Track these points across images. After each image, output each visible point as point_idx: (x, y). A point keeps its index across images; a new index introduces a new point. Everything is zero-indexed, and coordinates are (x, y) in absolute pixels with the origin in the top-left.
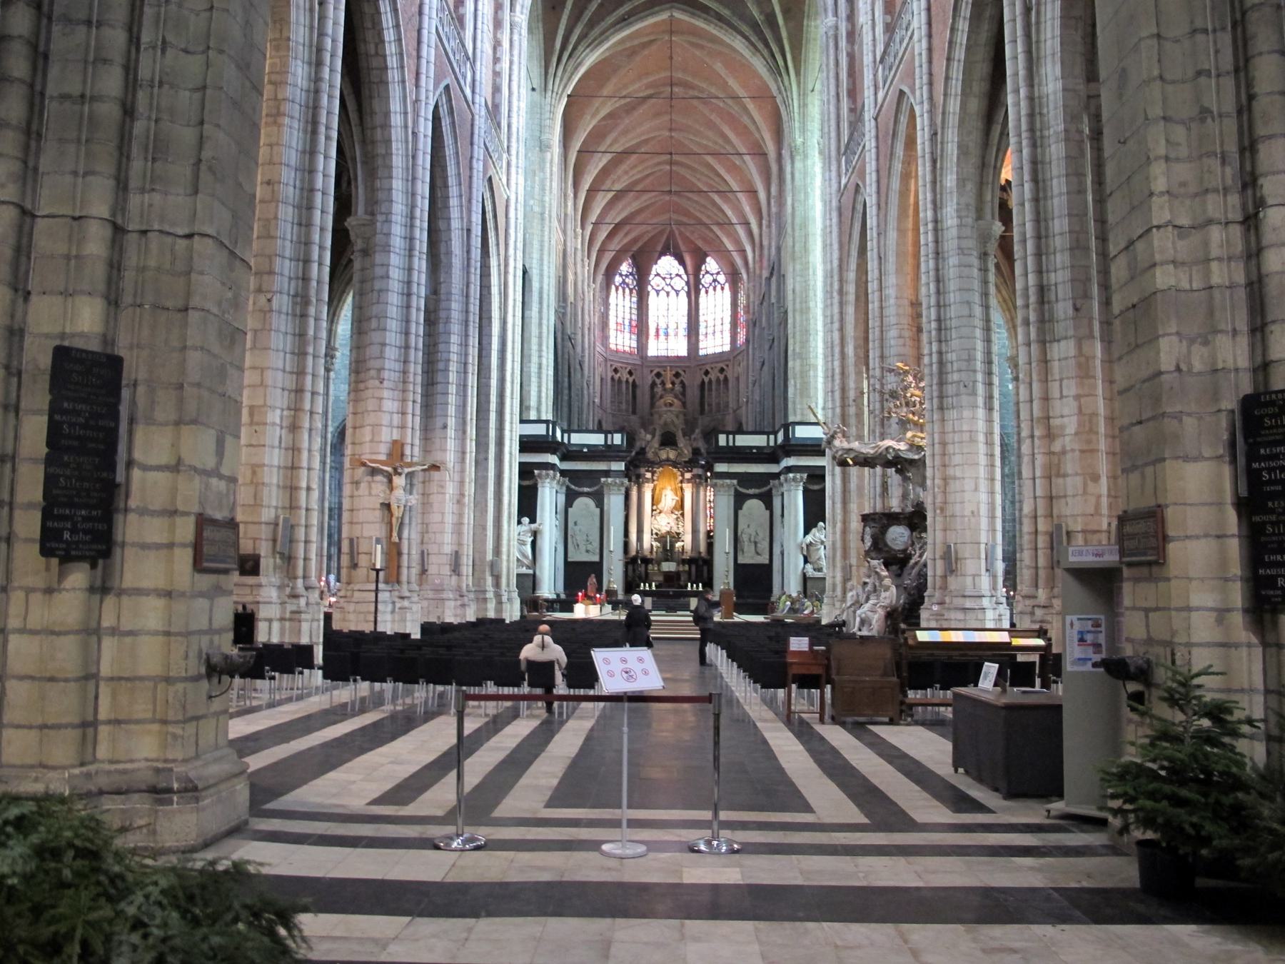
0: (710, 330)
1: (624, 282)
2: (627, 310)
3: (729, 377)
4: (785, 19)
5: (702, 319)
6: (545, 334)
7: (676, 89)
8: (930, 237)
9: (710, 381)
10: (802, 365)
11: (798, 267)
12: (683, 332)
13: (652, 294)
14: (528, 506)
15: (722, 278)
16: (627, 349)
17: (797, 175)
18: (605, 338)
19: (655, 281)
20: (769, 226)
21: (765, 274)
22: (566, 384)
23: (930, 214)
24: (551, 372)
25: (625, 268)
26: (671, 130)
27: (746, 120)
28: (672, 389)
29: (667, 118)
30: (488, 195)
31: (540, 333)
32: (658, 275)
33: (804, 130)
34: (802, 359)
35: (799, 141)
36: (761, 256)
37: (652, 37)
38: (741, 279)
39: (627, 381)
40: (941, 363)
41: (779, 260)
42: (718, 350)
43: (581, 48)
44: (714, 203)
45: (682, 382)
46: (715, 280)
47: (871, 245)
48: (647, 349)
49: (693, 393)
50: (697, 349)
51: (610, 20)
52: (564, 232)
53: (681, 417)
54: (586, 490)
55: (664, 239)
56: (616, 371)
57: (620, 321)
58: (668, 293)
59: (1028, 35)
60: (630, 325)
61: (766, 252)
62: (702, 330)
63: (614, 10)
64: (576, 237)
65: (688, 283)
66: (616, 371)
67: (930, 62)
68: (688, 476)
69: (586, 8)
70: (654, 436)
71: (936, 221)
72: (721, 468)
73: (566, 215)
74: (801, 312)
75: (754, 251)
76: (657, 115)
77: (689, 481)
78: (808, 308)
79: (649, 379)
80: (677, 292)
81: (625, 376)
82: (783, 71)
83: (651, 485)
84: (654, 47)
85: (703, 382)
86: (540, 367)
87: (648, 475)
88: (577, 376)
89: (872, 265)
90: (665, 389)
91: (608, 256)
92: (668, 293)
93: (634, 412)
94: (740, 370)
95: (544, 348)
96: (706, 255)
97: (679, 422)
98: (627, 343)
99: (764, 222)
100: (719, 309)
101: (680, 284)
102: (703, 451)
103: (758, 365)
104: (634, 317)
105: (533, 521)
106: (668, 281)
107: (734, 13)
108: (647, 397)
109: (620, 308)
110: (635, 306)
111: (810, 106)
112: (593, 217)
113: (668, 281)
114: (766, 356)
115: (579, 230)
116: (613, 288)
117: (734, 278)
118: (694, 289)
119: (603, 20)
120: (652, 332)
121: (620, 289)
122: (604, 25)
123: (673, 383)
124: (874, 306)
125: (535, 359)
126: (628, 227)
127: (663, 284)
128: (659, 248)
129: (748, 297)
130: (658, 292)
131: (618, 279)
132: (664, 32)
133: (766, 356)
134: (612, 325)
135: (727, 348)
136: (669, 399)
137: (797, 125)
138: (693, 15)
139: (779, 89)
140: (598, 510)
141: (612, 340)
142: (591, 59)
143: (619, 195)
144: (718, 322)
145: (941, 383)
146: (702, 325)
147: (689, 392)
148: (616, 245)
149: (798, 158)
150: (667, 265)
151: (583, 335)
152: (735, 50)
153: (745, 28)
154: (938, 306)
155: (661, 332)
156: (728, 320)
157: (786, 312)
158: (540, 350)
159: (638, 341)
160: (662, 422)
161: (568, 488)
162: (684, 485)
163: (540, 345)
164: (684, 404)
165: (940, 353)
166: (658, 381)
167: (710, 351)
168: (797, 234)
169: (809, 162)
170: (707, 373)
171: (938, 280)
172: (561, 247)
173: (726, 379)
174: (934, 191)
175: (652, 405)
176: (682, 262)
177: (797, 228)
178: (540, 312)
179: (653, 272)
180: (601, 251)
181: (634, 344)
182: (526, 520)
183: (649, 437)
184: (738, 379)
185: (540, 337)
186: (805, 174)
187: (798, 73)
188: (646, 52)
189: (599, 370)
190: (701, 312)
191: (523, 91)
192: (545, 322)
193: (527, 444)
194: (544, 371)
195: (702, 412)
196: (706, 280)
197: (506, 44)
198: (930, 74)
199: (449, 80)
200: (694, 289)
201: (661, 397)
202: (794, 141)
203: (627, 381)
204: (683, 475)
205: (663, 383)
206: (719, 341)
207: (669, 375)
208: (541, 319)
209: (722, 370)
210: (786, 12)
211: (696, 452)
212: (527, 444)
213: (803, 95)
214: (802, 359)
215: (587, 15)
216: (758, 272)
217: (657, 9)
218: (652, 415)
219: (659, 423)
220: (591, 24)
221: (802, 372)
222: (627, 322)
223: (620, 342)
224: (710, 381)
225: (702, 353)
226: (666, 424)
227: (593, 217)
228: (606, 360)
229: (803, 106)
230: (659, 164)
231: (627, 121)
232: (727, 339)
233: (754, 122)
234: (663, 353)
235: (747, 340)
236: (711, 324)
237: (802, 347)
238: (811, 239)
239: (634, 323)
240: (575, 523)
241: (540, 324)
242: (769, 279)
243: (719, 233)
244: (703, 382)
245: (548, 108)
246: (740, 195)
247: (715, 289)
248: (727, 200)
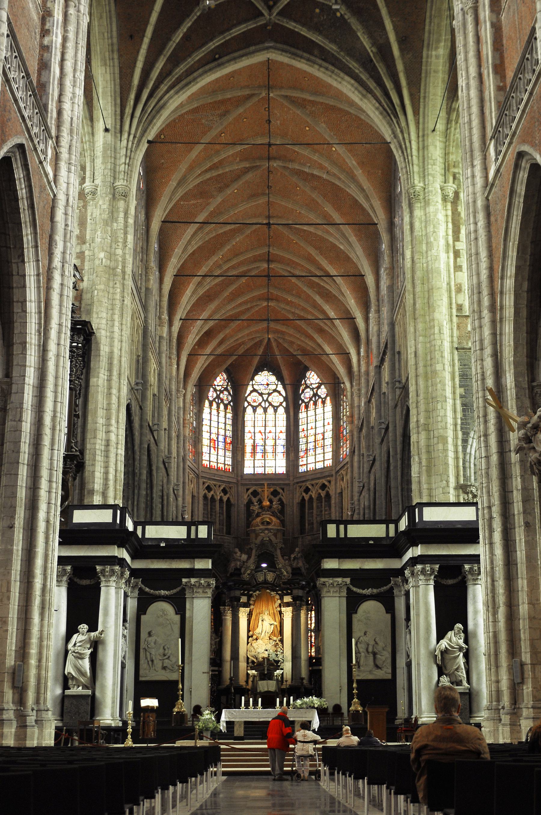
0: (311, 446)
1: (218, 397)
2: (222, 426)
3: (332, 493)
4: (401, 50)
5: (301, 435)
6: (114, 407)
7: (275, 164)
9: (311, 498)
10: (428, 439)
11: (420, 326)
12: (281, 449)
13: (249, 410)
15: (323, 392)
16: (221, 466)
17: (417, 225)
18: (198, 454)
20: (378, 311)
21: (375, 362)
22: (144, 477)
24: (122, 451)
25: (220, 381)
26: (269, 217)
28: (270, 507)
29: (262, 200)
31: (109, 404)
32: (254, 390)
33: (424, 175)
34: (428, 430)
35: (419, 185)
36: (367, 351)
37: (247, 92)
38: (344, 390)
39: (221, 500)
41: (393, 336)
42: (320, 465)
44: (315, 306)
45: (280, 500)
46: (315, 395)
48: (243, 466)
49: (293, 511)
50: (297, 466)
52: (145, 307)
53: (279, 535)
54: (163, 592)
55: (260, 351)
56: (209, 488)
57: (214, 437)
58: (265, 410)
60: (225, 441)
61: (374, 346)
62: (302, 447)
63: (203, 45)
64: (161, 325)
65: (286, 399)
66: (209, 488)
68: (287, 599)
69: (169, 39)
70: (249, 558)
72: (330, 564)
73: (147, 289)
74: (426, 379)
75: (359, 353)
76: (254, 196)
77: (288, 605)
78: (435, 372)
79: (245, 498)
80: (276, 409)
81: (219, 495)
82: (398, 109)
83: (248, 610)
84: (249, 104)
85: (303, 499)
86: (108, 445)
87: (244, 599)
88: (159, 476)
90: (262, 507)
91: (201, 363)
92: (265, 410)
93: (229, 533)
94: (344, 484)
95: (113, 422)
96: (307, 369)
98: (221, 460)
99: (372, 315)
100: (320, 424)
101: (276, 399)
102: (303, 570)
103: (366, 467)
104: (229, 434)
106: (265, 397)
107: (341, 48)
108: (243, 516)
109: (214, 424)
110: (229, 422)
111: (431, 148)
113: (265, 397)
114: (377, 452)
115: (165, 317)
116: (207, 403)
119: (190, 56)
120: (248, 449)
121: (215, 405)
122: (191, 61)
123: (271, 501)
125: (101, 435)
126: (221, 336)
127: (260, 399)
128: (256, 360)
129: (352, 407)
130: (255, 409)
131: (212, 394)
132: (260, 87)
133: (377, 452)
134: (206, 441)
135: (329, 463)
136: (267, 517)
137: (416, 169)
138: (294, 55)
139: (394, 133)
140: (177, 618)
141: (205, 457)
144: (320, 437)
146: (302, 441)
147: (288, 510)
149: (417, 205)
151: (170, 438)
152: (339, 95)
153: (353, 65)
155: (259, 449)
156: (329, 435)
157: (405, 389)
158: (108, 425)
159: (234, 458)
160: (258, 541)
161: (140, 590)
162: (283, 609)
163: (108, 419)
164: (283, 522)
166: (255, 500)
167: (311, 467)
168: (418, 289)
169: (431, 209)
170: (307, 490)
172: (139, 322)
173: (328, 495)
175: (248, 524)
176: (280, 378)
177: (418, 282)
178: (109, 380)
179: (250, 388)
180: (192, 356)
181: (229, 461)
183: (244, 557)
184: (341, 493)
185: (108, 409)
186: (427, 222)
187: (416, 113)
188: (241, 110)
189: (191, 487)
190: (301, 428)
192: (114, 391)
194: (112, 450)
195: (302, 531)
201: (258, 515)
202: (413, 187)
203: (221, 500)
204: (281, 599)
205: (260, 502)
206: (320, 458)
207: (266, 493)
208: (110, 388)
209: (323, 487)
210: (402, 41)
211: (296, 572)
213: (422, 137)
214: (428, 430)
215: (171, 46)
216: (363, 369)
217: (252, 48)
218: (248, 535)
221: (428, 446)
222: (221, 439)
223: (213, 458)
224: (311, 498)
225: (302, 469)
226: (263, 543)
228: (198, 476)
229: (423, 148)
230: (256, 259)
231: (219, 199)
232: (329, 456)
233: (363, 190)
234: (260, 471)
235: (353, 452)
236: (311, 439)
237: (428, 418)
238: (436, 295)
239: (229, 440)
240: (150, 634)
241: (109, 394)
242: (379, 367)
243: (320, 340)
244: (303, 499)
245: (123, 152)
246: (337, 322)
247: (315, 404)
248: (328, 296)
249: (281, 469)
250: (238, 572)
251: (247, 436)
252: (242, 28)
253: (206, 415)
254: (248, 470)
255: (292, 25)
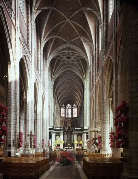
8: (102, 101)
12: (71, 114)
14: (50, 137)
15: (76, 107)
19: (67, 108)
23: (102, 98)
25: (63, 105)
27: (79, 85)
30: (43, 95)
40: (103, 118)
43: (56, 74)
47: (95, 102)
51: (60, 70)
59: (116, 71)
67: (103, 75)
71: (103, 98)
81: (63, 120)
89: (95, 105)
97: (70, 126)
101: (70, 108)
105: (51, 139)
112: (59, 99)
117: (77, 107)
118: (72, 109)
120: (67, 114)
124: (95, 111)
131: (62, 107)
134: (62, 113)
141: (62, 116)
142: (57, 76)
143: (62, 96)
145: (103, 121)
148: (62, 103)
150: (69, 105)
154: (103, 110)
156: (77, 113)
159: (65, 115)
165: (103, 117)
171: (103, 107)
174: (103, 94)
176: (71, 105)
182: (50, 139)
191: (48, 80)
193: (50, 129)
196: (74, 107)
197: (45, 73)
198: (103, 77)
199: (37, 78)
200: (72, 109)
207: (69, 120)
210: (84, 69)
212: (50, 129)
215: (57, 69)
219: (68, 126)
220: (57, 71)
227: (59, 99)
234: (68, 117)
249: (71, 117)
250: (66, 130)
251: (67, 113)
252: (65, 66)
253: (62, 110)
254: (67, 117)
255: (71, 66)
